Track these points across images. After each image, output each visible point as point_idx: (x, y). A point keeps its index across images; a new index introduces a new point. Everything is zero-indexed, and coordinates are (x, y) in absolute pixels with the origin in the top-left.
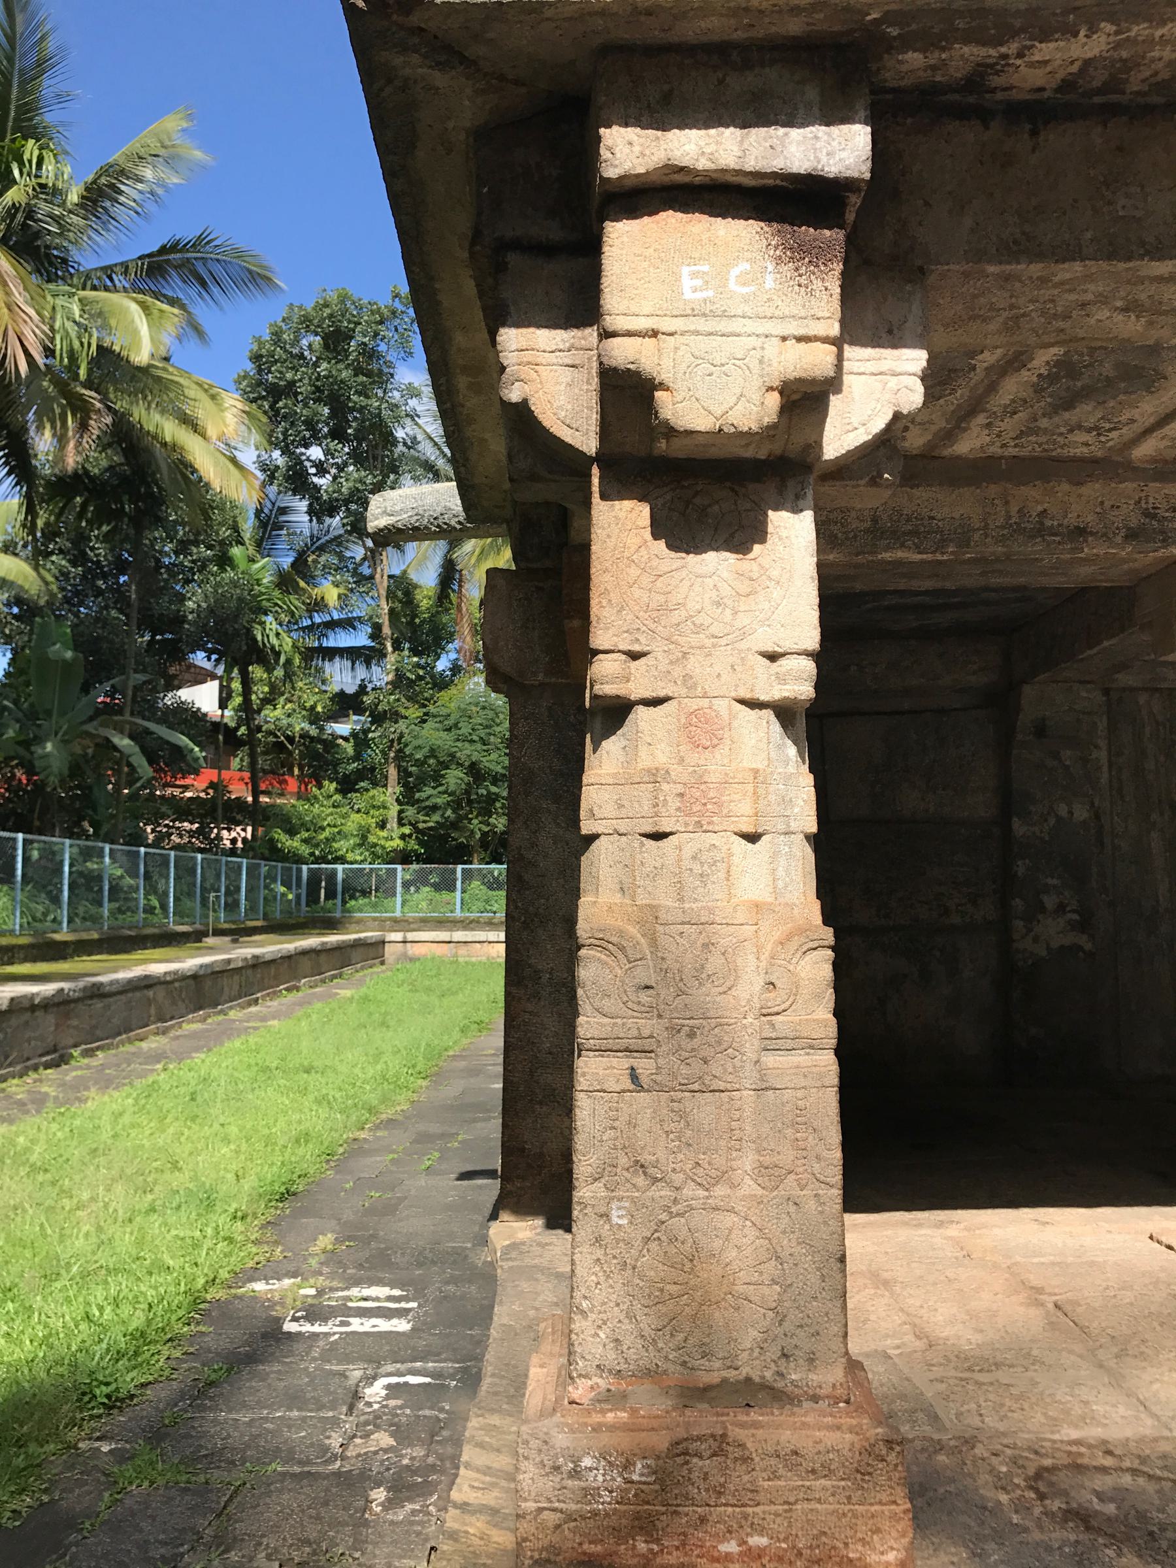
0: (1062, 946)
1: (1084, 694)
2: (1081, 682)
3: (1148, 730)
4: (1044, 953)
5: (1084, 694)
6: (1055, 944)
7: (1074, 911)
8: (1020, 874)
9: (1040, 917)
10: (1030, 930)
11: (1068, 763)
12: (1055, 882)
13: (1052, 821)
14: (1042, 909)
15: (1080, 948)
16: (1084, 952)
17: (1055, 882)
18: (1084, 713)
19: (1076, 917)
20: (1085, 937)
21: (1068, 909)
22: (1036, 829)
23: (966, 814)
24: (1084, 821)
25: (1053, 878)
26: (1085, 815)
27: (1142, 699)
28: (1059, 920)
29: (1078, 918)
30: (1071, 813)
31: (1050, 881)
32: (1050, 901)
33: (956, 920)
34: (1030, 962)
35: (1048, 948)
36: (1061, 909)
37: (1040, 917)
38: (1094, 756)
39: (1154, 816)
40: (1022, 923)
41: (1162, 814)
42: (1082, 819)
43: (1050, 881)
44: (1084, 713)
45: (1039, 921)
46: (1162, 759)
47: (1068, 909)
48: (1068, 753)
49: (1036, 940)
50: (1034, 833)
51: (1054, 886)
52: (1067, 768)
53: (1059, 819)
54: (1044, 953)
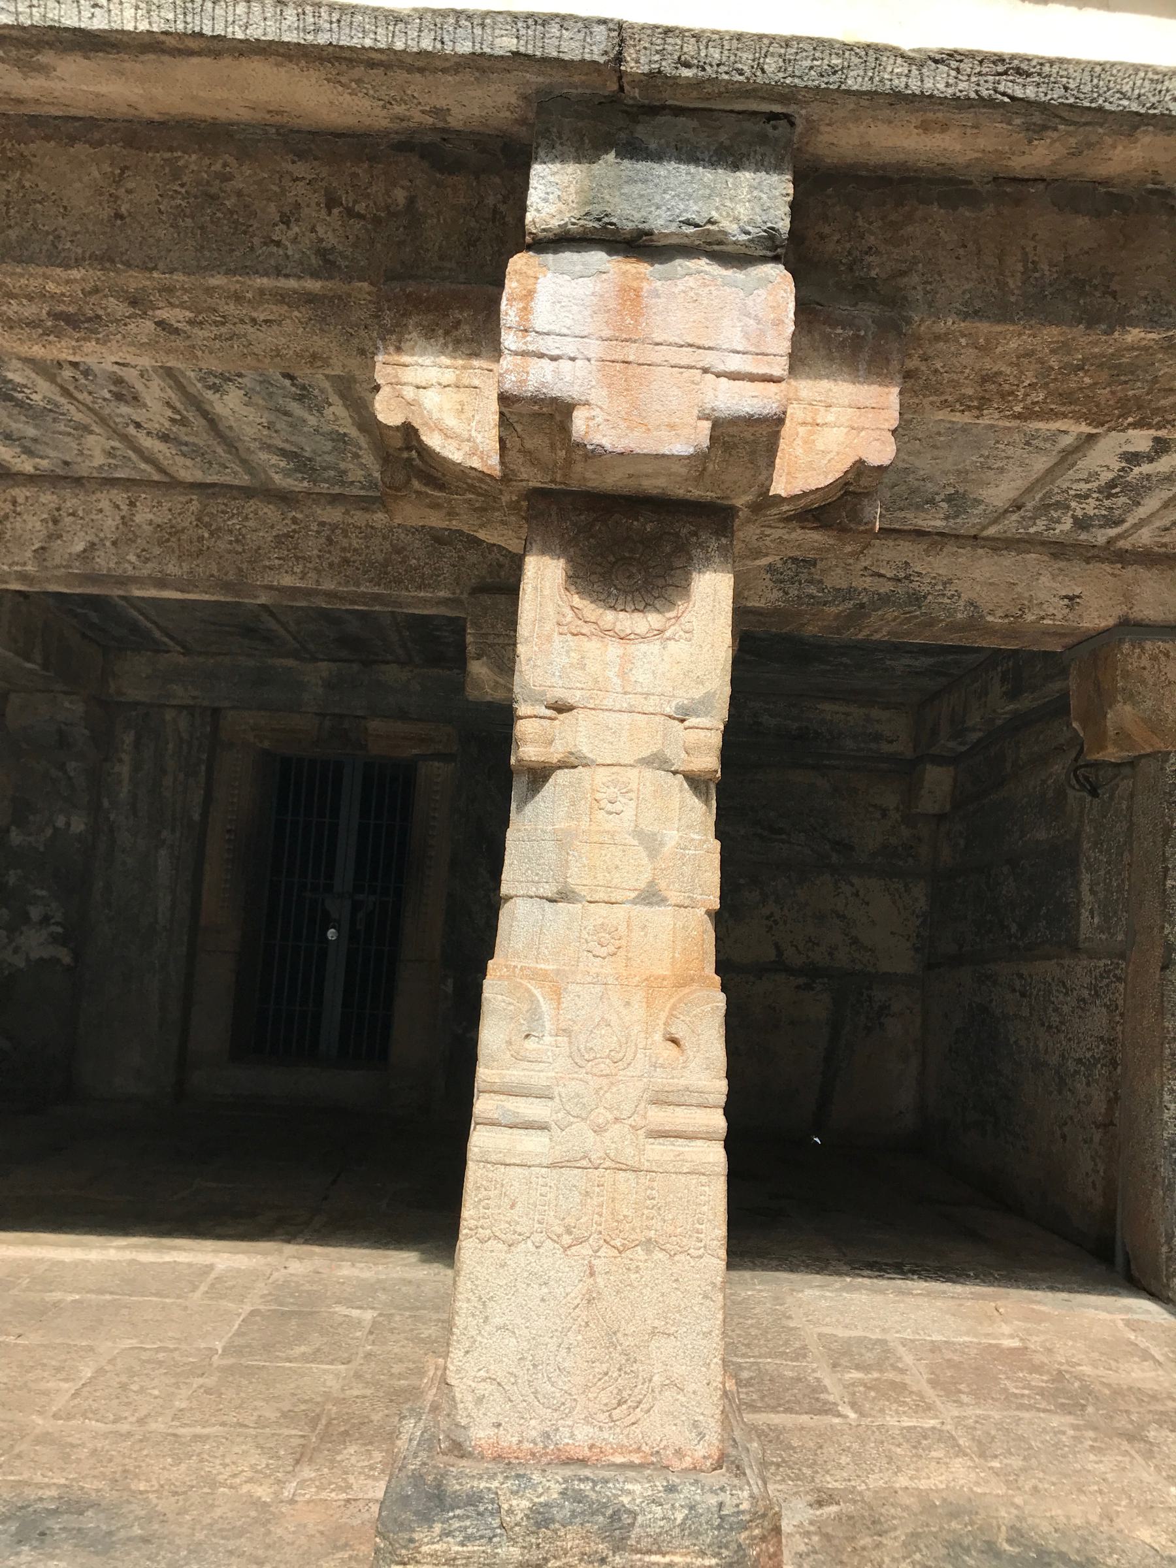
0: (41, 959)
1: (67, 704)
2: (65, 693)
3: (170, 746)
4: (22, 965)
5: (67, 704)
6: (34, 955)
7: (57, 924)
8: (11, 883)
11: (72, 774)
12: (44, 893)
13: (49, 832)
14: (26, 918)
15: (58, 961)
17: (44, 893)
18: (66, 724)
19: (60, 930)
21: (53, 921)
22: (31, 839)
24: (80, 833)
25: (42, 888)
26: (82, 827)
27: (169, 715)
29: (60, 930)
30: (68, 824)
31: (40, 893)
32: (35, 913)
35: (28, 959)
36: (46, 920)
37: (24, 928)
38: (116, 769)
39: (165, 834)
41: (173, 830)
42: (78, 831)
46: (181, 776)
47: (53, 921)
48: (74, 764)
49: (16, 951)
52: (70, 778)
53: (56, 829)
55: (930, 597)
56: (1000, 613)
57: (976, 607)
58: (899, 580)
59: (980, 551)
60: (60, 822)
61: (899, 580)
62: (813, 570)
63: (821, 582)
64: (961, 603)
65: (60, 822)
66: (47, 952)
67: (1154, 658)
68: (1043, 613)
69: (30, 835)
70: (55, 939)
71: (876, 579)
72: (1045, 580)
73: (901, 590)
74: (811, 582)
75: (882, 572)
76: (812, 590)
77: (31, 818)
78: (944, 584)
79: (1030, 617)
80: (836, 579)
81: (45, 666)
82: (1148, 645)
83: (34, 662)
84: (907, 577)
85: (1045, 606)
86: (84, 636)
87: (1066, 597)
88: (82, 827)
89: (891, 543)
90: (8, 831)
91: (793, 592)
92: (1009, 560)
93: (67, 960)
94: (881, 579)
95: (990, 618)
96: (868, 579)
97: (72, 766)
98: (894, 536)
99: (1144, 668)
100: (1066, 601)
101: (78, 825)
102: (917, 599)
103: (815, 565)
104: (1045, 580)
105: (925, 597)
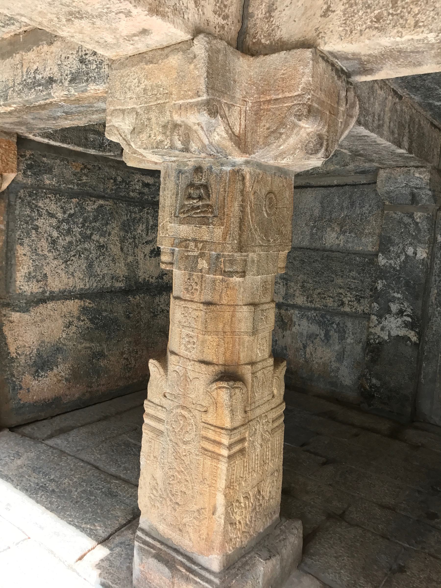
0: (398, 336)
1: (417, 175)
2: (417, 167)
4: (386, 338)
5: (417, 175)
6: (394, 333)
7: (408, 316)
8: (379, 288)
9: (387, 316)
10: (380, 323)
11: (418, 220)
12: (399, 296)
13: (403, 258)
14: (389, 311)
16: (411, 341)
17: (399, 296)
18: (416, 188)
19: (410, 320)
20: (413, 333)
21: (405, 313)
23: (361, 248)
24: (423, 259)
25: (398, 293)
26: (425, 255)
28: (399, 319)
29: (410, 320)
30: (415, 253)
31: (396, 295)
32: (394, 307)
33: (347, 309)
34: (377, 341)
35: (389, 335)
36: (401, 313)
37: (387, 316)
40: (376, 318)
42: (422, 257)
43: (396, 295)
44: (416, 188)
45: (386, 318)
47: (405, 313)
48: (419, 214)
49: (382, 329)
50: (391, 264)
51: (399, 299)
52: (417, 223)
53: (407, 256)
54: (386, 338)
60: (410, 251)
65: (410, 251)
66: (402, 332)
69: (391, 259)
70: (406, 325)
77: (391, 248)
81: (410, 151)
83: (404, 148)
86: (432, 124)
88: (425, 255)
90: (377, 255)
93: (414, 339)
97: (418, 215)
101: (422, 254)
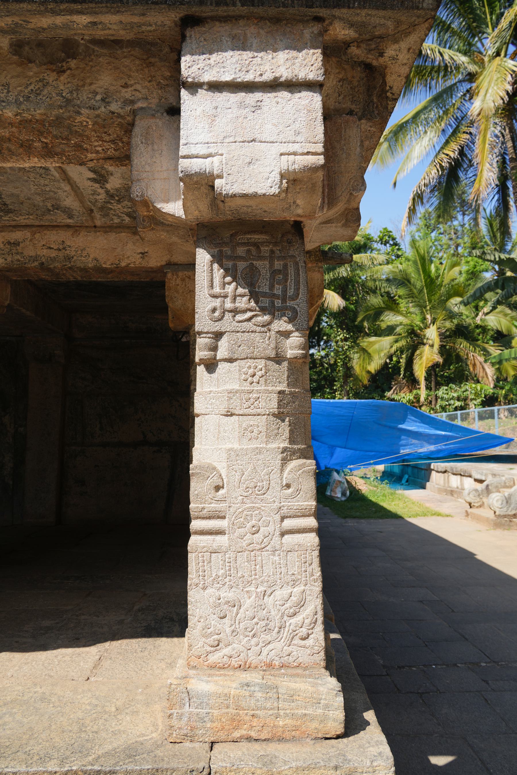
55: (75, 258)
56: (109, 263)
57: (97, 261)
58: (60, 250)
59: (98, 233)
61: (60, 250)
62: (18, 248)
63: (22, 253)
64: (90, 259)
67: (183, 280)
68: (129, 262)
71: (49, 250)
72: (130, 246)
73: (61, 254)
74: (17, 253)
75: (52, 246)
76: (19, 257)
78: (82, 250)
79: (123, 264)
80: (30, 252)
82: (180, 274)
84: (64, 248)
85: (130, 258)
87: (141, 253)
89: (55, 232)
91: (9, 259)
92: (112, 236)
94: (52, 250)
95: (104, 266)
96: (45, 251)
98: (56, 229)
99: (178, 285)
100: (141, 255)
102: (69, 259)
103: (19, 245)
104: (130, 246)
105: (73, 257)
